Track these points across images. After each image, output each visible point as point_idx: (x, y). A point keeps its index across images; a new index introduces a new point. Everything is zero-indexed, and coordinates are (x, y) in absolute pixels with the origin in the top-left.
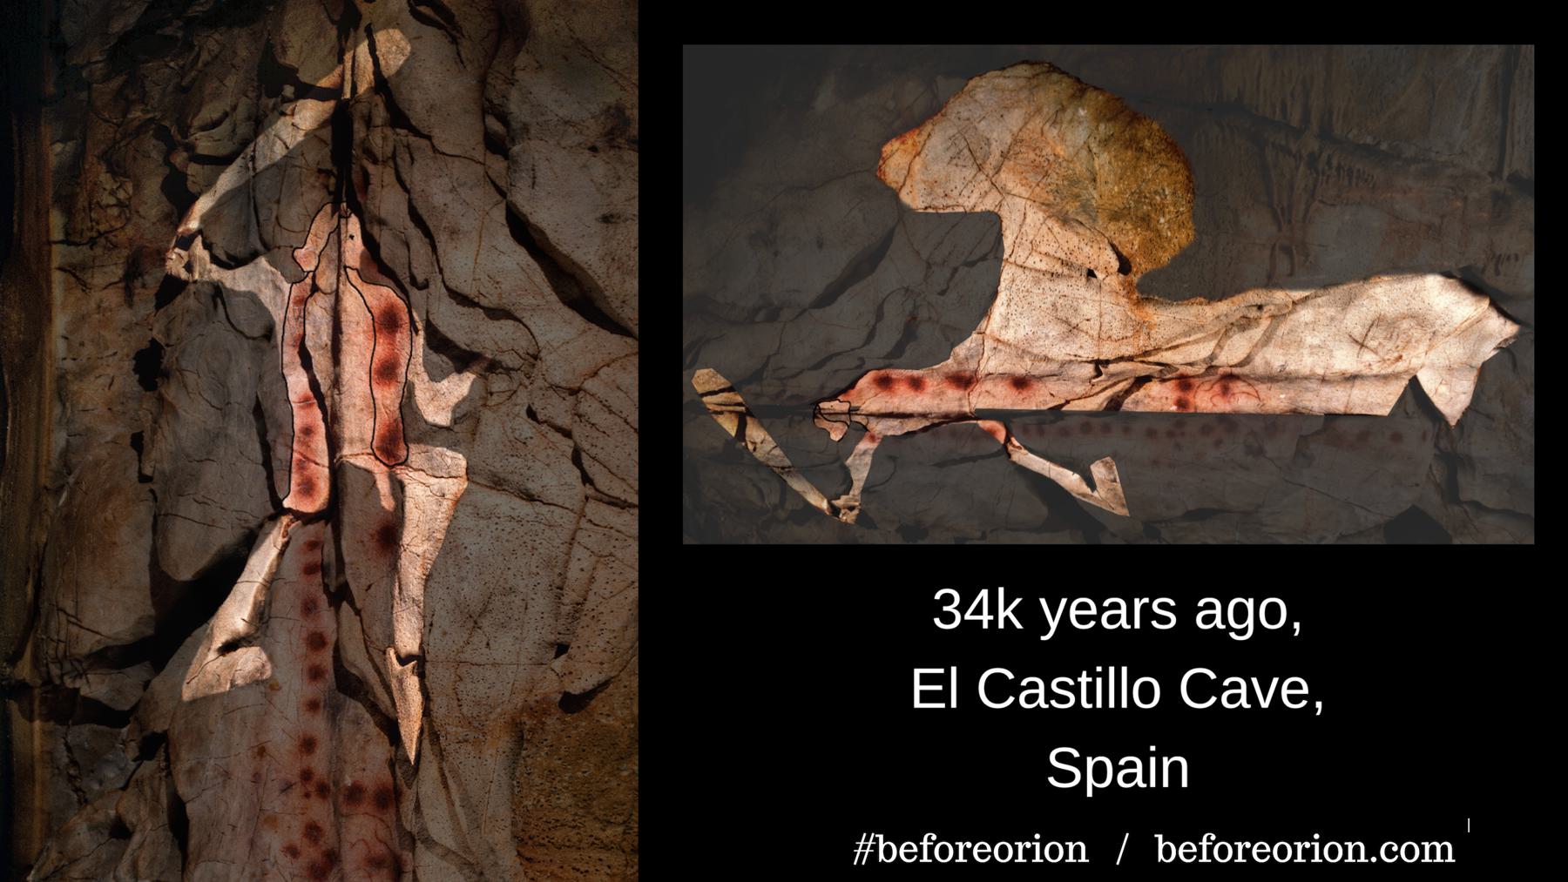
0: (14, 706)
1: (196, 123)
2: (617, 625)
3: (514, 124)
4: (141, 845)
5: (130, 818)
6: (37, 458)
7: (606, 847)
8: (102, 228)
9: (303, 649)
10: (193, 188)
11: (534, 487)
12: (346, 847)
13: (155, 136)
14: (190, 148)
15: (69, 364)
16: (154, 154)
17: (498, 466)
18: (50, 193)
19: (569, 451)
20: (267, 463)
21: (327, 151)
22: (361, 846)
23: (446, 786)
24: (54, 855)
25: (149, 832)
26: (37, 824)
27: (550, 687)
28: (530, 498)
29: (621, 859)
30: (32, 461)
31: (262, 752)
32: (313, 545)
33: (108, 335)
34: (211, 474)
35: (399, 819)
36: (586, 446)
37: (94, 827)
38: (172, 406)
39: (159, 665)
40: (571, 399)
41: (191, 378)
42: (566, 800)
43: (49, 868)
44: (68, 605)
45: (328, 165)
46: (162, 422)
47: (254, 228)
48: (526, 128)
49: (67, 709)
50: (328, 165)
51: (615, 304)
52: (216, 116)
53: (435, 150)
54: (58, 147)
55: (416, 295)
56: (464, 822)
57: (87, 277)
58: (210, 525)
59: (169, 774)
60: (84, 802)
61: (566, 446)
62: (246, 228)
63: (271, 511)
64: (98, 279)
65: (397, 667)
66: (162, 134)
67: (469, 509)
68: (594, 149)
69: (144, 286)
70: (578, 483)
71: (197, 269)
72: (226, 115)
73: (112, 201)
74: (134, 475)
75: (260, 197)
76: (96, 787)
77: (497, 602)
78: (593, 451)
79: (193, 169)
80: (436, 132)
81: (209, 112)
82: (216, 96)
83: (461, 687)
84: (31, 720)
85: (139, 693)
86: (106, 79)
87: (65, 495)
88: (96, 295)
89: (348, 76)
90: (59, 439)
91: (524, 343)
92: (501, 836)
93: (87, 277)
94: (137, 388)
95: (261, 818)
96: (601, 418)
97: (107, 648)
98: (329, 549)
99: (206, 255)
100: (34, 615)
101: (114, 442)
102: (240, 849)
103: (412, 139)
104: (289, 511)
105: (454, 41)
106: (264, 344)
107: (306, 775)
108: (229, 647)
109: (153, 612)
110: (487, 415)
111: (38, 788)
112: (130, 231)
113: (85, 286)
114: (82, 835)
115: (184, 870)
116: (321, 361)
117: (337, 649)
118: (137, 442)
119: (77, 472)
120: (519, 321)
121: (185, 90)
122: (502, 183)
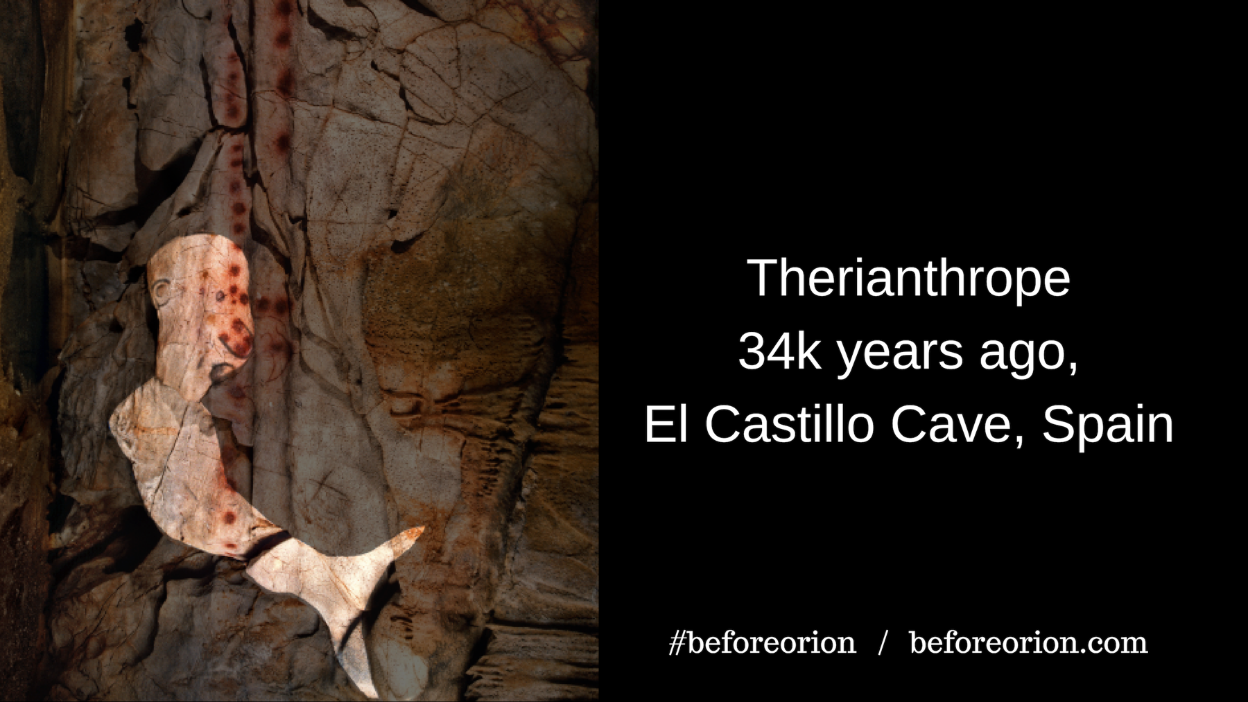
0: (49, 250)
2: (427, 198)
4: (129, 336)
5: (123, 319)
6: (64, 93)
7: (420, 338)
9: (230, 213)
11: (375, 112)
15: (84, 35)
17: (353, 98)
19: (398, 89)
20: (208, 97)
22: (267, 337)
23: (321, 300)
24: (75, 342)
25: (134, 328)
26: (64, 323)
27: (386, 237)
28: (373, 118)
30: (60, 95)
33: (108, 16)
35: (291, 320)
36: (408, 86)
38: (149, 62)
39: (140, 224)
40: (399, 57)
41: (160, 44)
42: (395, 308)
43: (71, 351)
44: (84, 186)
46: (142, 71)
49: (82, 250)
56: (331, 321)
58: (174, 135)
60: (93, 309)
61: (396, 86)
63: (211, 126)
65: (290, 225)
67: (335, 126)
70: (403, 109)
74: (124, 103)
76: (101, 300)
77: (352, 184)
78: (413, 89)
83: (330, 237)
84: (60, 258)
85: (128, 241)
87: (81, 116)
90: (78, 82)
91: (369, 22)
92: (355, 331)
94: (127, 49)
96: (417, 68)
98: (247, 150)
100: (62, 189)
101: (113, 83)
106: (206, 22)
108: (185, 212)
109: (136, 190)
110: (346, 67)
111: (65, 301)
114: (92, 330)
116: (242, 33)
118: (127, 83)
119: (89, 102)
120: (366, 7)
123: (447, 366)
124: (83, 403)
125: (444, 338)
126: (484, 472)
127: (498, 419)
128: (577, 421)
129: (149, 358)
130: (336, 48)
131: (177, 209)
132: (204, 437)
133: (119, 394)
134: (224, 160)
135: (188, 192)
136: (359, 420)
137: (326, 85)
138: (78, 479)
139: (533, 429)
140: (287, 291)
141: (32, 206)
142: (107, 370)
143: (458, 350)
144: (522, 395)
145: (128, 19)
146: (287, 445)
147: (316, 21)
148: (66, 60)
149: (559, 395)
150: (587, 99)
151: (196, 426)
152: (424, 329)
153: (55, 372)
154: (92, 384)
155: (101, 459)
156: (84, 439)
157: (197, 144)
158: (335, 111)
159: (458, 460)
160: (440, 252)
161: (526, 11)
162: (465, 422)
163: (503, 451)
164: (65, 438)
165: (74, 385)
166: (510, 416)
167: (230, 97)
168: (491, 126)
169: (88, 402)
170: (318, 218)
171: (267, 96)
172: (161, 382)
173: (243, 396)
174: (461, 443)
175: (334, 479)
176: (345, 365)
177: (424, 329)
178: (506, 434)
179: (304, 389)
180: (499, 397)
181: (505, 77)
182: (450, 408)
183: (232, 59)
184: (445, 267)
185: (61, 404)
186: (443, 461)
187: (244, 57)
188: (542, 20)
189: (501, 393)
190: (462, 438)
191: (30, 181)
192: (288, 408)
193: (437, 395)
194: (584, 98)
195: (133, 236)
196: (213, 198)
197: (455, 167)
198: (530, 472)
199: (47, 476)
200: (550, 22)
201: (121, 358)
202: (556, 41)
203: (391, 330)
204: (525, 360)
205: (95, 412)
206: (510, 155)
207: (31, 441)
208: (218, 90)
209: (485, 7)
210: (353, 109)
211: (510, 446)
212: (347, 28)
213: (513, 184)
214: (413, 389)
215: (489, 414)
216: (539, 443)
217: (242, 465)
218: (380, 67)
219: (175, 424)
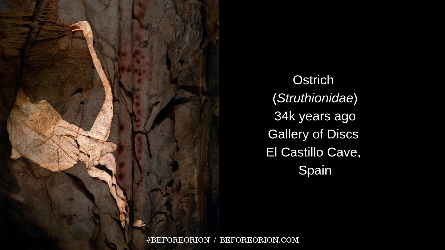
0: (206, 90)
1: (165, 221)
2: (70, 108)
3: (93, 221)
4: (177, 58)
5: (179, 65)
6: (201, 146)
7: (72, 58)
8: (186, 198)
10: (165, 206)
11: (88, 139)
12: (131, 58)
13: (174, 218)
14: (166, 216)
15: (193, 167)
16: (174, 214)
17: (96, 144)
18: (198, 205)
20: (149, 145)
21: (135, 215)
22: (127, 58)
23: (108, 72)
24: (197, 56)
25: (175, 62)
27: (85, 94)
28: (89, 137)
29: (69, 55)
30: (202, 145)
31: (150, 80)
32: (138, 126)
34: (161, 142)
35: (119, 65)
36: (76, 149)
37: (188, 62)
38: (170, 158)
39: (173, 99)
40: (80, 159)
41: (166, 164)
42: (81, 69)
43: (198, 53)
44: (194, 113)
45: (135, 212)
46: (172, 154)
47: (152, 198)
48: (90, 220)
49: (194, 89)
50: (135, 212)
51: (70, 180)
52: (160, 223)
53: (111, 215)
54: (196, 216)
55: (115, 183)
57: (189, 187)
58: (161, 131)
59: (171, 75)
60: (190, 68)
61: (81, 149)
62: (153, 197)
63: (148, 134)
64: (187, 186)
65: (119, 99)
66: (172, 219)
68: (75, 215)
69: (176, 184)
71: (164, 188)
72: (158, 223)
73: (184, 204)
74: (179, 142)
75: (150, 204)
76: (187, 72)
78: (75, 148)
79: (165, 211)
80: (110, 219)
81: (162, 223)
82: (160, 227)
84: (202, 87)
86: (185, 231)
88: (187, 182)
89: (130, 232)
90: (196, 150)
93: (189, 187)
94: (178, 161)
95: (150, 65)
96: (73, 155)
97: (185, 103)
98: (135, 125)
99: (162, 191)
101: (183, 149)
102: (155, 58)
103: (116, 217)
104: (144, 134)
105: (106, 240)
106: (149, 171)
107: (140, 74)
108: (157, 103)
110: (99, 156)
111: (200, 71)
112: (180, 197)
113: (190, 184)
114: (191, 61)
115: (167, 53)
116: (136, 167)
117: (133, 103)
118: (178, 149)
119: (192, 143)
121: (167, 229)
122: (96, 208)
123: (63, 48)
124: (194, 35)
125: (64, 58)
126: (49, 10)
127: (44, 29)
128: (16, 28)
129: (170, 51)
130: (102, 163)
131: (160, 104)
132: (150, 22)
133: (180, 38)
134: (143, 122)
135: (156, 110)
136: (94, 28)
137: (106, 149)
138: (195, 8)
139: (32, 25)
140: (120, 75)
141: (212, 105)
142: (185, 47)
143: (58, 54)
144: (36, 37)
145: (177, 172)
146: (120, 19)
147: (110, 172)
148: (200, 158)
149: (22, 38)
150: (12, 144)
151: (153, 26)
152: (70, 61)
153: (204, 46)
154: (190, 42)
155: (187, 15)
156: (193, 22)
157: (153, 127)
158: (103, 140)
159: (59, 14)
160: (65, 89)
161: (34, 175)
162: (56, 28)
163: (42, 18)
164: (200, 22)
165: (197, 41)
166: (40, 30)
167: (141, 144)
168: (47, 135)
169: (192, 35)
170: (109, 101)
171: (127, 145)
172: (166, 42)
173: (136, 37)
174: (58, 20)
175: (103, 7)
176: (99, 48)
177: (70, 61)
178: (41, 23)
179: (114, 40)
180: (44, 37)
181: (42, 152)
182: (62, 33)
183: (140, 158)
184: (63, 83)
185: (202, 34)
186: (64, 14)
187: (136, 159)
188: (28, 172)
189: (43, 38)
190: (57, 22)
191: (213, 114)
192: (120, 33)
193: (66, 38)
194: (13, 145)
195: (176, 95)
196: (147, 108)
197: (60, 120)
198: (33, 10)
199: (207, 9)
200: (26, 171)
201: (180, 51)
202: (23, 164)
203: (83, 61)
204: (34, 50)
205: (189, 31)
206: (39, 124)
207: (213, 21)
208: (145, 147)
209: (49, 177)
210: (96, 140)
211: (40, 19)
212: (98, 170)
213: (39, 113)
214: (75, 39)
215: (47, 31)
216: (30, 20)
217: (136, 12)
218: (87, 155)
219: (161, 27)
